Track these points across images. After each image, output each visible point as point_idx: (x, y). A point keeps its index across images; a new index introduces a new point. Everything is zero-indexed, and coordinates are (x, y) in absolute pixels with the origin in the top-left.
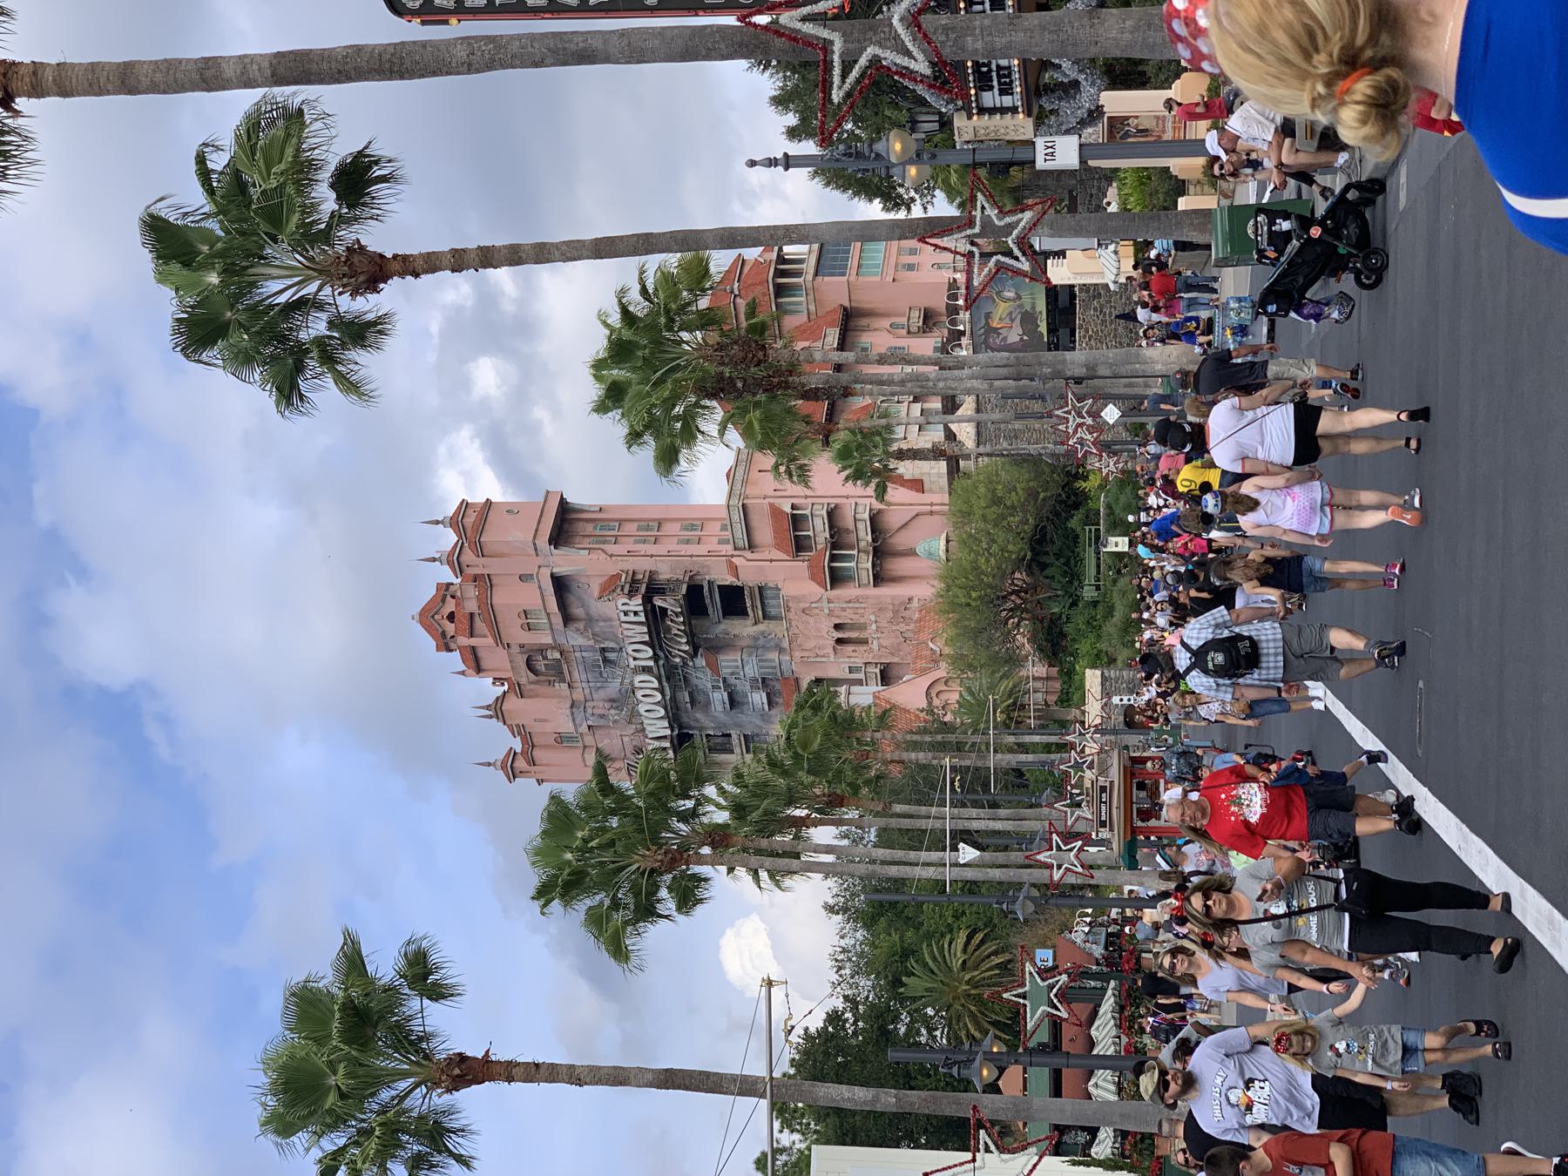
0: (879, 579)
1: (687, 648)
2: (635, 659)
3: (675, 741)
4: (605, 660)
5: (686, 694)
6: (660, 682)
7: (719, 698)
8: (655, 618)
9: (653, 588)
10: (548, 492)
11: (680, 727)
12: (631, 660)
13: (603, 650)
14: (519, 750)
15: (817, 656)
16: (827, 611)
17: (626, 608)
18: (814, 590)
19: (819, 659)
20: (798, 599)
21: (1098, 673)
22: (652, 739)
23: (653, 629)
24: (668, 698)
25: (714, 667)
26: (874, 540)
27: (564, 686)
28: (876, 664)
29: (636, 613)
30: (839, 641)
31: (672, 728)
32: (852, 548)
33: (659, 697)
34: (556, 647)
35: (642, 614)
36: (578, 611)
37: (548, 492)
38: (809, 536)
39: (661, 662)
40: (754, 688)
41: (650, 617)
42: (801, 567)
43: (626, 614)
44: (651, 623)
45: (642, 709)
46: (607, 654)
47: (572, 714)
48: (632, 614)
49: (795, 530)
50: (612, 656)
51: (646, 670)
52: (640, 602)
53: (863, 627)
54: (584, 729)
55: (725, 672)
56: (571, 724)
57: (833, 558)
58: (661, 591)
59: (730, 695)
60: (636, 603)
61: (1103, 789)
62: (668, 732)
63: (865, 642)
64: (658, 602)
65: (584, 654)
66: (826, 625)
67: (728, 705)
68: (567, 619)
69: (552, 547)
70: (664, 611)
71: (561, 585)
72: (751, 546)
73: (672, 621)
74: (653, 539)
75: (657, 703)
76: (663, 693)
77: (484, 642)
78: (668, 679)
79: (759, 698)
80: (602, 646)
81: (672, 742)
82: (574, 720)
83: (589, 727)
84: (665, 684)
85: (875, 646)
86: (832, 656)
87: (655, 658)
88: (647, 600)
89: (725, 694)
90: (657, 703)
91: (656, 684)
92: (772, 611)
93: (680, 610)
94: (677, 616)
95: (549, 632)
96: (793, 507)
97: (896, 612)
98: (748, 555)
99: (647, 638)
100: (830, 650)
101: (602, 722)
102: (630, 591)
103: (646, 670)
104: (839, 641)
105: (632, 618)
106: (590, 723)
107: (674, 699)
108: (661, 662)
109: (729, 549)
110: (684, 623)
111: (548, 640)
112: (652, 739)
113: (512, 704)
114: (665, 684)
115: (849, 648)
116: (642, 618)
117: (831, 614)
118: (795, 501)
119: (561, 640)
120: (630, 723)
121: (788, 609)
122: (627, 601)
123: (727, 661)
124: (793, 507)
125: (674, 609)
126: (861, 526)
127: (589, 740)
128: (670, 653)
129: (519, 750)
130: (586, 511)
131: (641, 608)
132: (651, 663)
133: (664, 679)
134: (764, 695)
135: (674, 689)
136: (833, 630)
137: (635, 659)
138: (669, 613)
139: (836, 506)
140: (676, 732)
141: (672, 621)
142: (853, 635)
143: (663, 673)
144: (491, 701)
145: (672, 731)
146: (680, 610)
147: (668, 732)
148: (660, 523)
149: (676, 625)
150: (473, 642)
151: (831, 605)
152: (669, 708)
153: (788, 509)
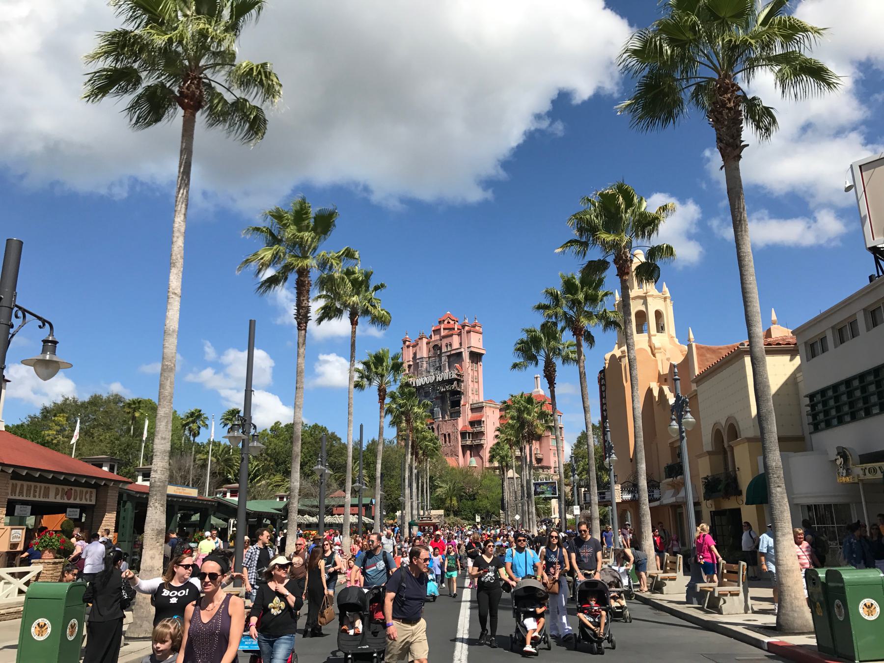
0: (464, 448)
8: (450, 381)
9: (459, 381)
18: (460, 427)
20: (457, 423)
21: (443, 514)
30: (445, 435)
31: (419, 386)
36: (451, 359)
51: (436, 379)
53: (450, 442)
57: (469, 433)
58: (458, 384)
60: (454, 376)
61: (430, 518)
64: (455, 383)
66: (449, 431)
88: (456, 379)
92: (453, 415)
96: (483, 421)
97: (454, 452)
103: (436, 379)
104: (445, 435)
109: (471, 402)
121: (454, 420)
124: (483, 421)
126: (479, 441)
142: (447, 439)
150: (442, 330)
153: (482, 420)
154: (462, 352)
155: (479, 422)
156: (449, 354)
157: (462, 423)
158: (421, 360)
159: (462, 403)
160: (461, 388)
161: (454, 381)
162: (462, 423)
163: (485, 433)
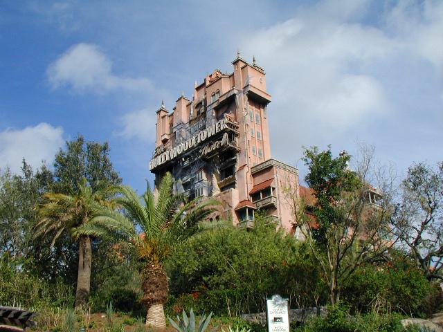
9: (232, 135)
18: (235, 203)
20: (230, 198)
29: (219, 128)
31: (174, 158)
38: (260, 198)
42: (246, 196)
58: (230, 137)
64: (226, 135)
72: (254, 175)
76: (187, 151)
78: (193, 153)
81: (168, 161)
88: (224, 131)
98: (249, 174)
113: (184, 103)
118: (276, 189)
124: (274, 189)
131: (222, 129)
139: (276, 209)
140: (172, 162)
154: (234, 95)
155: (267, 191)
156: (215, 105)
157: (237, 196)
158: (179, 127)
159: (237, 167)
160: (234, 144)
162: (237, 196)
163: (277, 206)
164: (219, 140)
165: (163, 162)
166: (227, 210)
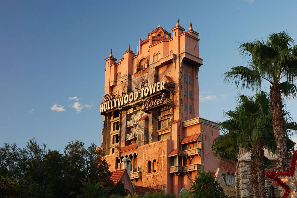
1: (147, 107)
2: (144, 90)
3: (117, 109)
4: (144, 83)
5: (132, 112)
6: (137, 100)
7: (130, 123)
10: (202, 60)
11: (121, 110)
12: (143, 89)
13: (148, 82)
14: (116, 62)
15: (145, 155)
16: (160, 156)
17: (161, 84)
19: (143, 155)
22: (117, 101)
23: (154, 95)
24: (131, 104)
25: (140, 120)
26: (187, 173)
27: (136, 71)
28: (142, 177)
29: (159, 88)
31: (121, 107)
32: (184, 165)
33: (131, 100)
34: (148, 66)
35: (159, 90)
37: (202, 60)
39: (143, 100)
40: (134, 135)
41: (158, 93)
43: (159, 85)
44: (156, 94)
45: (127, 96)
46: (146, 84)
47: (126, 75)
48: (159, 87)
49: (191, 143)
50: (146, 85)
51: (139, 96)
52: (164, 88)
54: (122, 80)
55: (140, 122)
56: (123, 75)
59: (132, 127)
60: (163, 87)
62: (119, 106)
63: (149, 171)
65: (146, 76)
67: (128, 127)
68: (157, 69)
69: (183, 59)
70: (160, 98)
71: (169, 63)
73: (156, 101)
74: (186, 95)
75: (129, 101)
76: (133, 101)
77: (150, 43)
78: (137, 104)
79: (130, 137)
80: (149, 81)
82: (125, 76)
83: (122, 82)
84: (135, 102)
85: (148, 176)
86: (145, 160)
87: (144, 97)
88: (163, 91)
89: (132, 125)
90: (129, 101)
91: (135, 99)
93: (161, 103)
94: (158, 103)
95: (153, 63)
99: (151, 93)
100: (147, 158)
101: (124, 86)
102: (167, 85)
104: (149, 162)
105: (158, 86)
106: (123, 81)
107: (130, 107)
108: (143, 100)
110: (156, 105)
111: (151, 62)
112: (117, 101)
114: (135, 102)
115: (147, 166)
116: (158, 90)
117: (160, 158)
119: (151, 67)
120: (123, 93)
122: (164, 84)
123: (143, 123)
125: (161, 101)
127: (119, 83)
128: (146, 102)
129: (116, 62)
130: (196, 74)
132: (142, 96)
133: (137, 102)
134: (132, 138)
135: (134, 107)
136: (154, 159)
137: (144, 90)
138: (159, 99)
140: (119, 109)
141: (156, 101)
143: (139, 101)
144: (131, 50)
145: (120, 107)
146: (161, 103)
147: (119, 106)
148: (192, 99)
149: (156, 103)
151: (163, 158)
152: (127, 105)
161: (161, 94)
164: (158, 98)
165: (112, 108)
166: (162, 156)
